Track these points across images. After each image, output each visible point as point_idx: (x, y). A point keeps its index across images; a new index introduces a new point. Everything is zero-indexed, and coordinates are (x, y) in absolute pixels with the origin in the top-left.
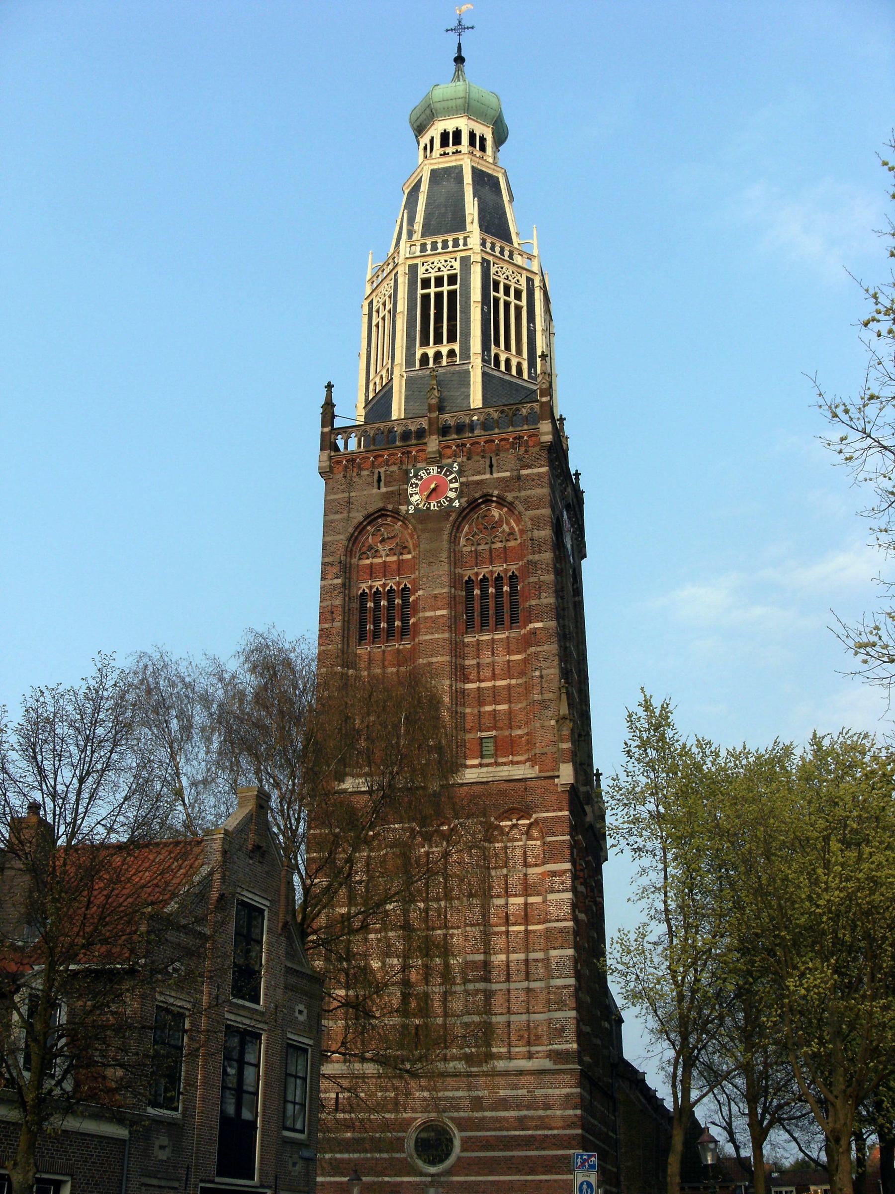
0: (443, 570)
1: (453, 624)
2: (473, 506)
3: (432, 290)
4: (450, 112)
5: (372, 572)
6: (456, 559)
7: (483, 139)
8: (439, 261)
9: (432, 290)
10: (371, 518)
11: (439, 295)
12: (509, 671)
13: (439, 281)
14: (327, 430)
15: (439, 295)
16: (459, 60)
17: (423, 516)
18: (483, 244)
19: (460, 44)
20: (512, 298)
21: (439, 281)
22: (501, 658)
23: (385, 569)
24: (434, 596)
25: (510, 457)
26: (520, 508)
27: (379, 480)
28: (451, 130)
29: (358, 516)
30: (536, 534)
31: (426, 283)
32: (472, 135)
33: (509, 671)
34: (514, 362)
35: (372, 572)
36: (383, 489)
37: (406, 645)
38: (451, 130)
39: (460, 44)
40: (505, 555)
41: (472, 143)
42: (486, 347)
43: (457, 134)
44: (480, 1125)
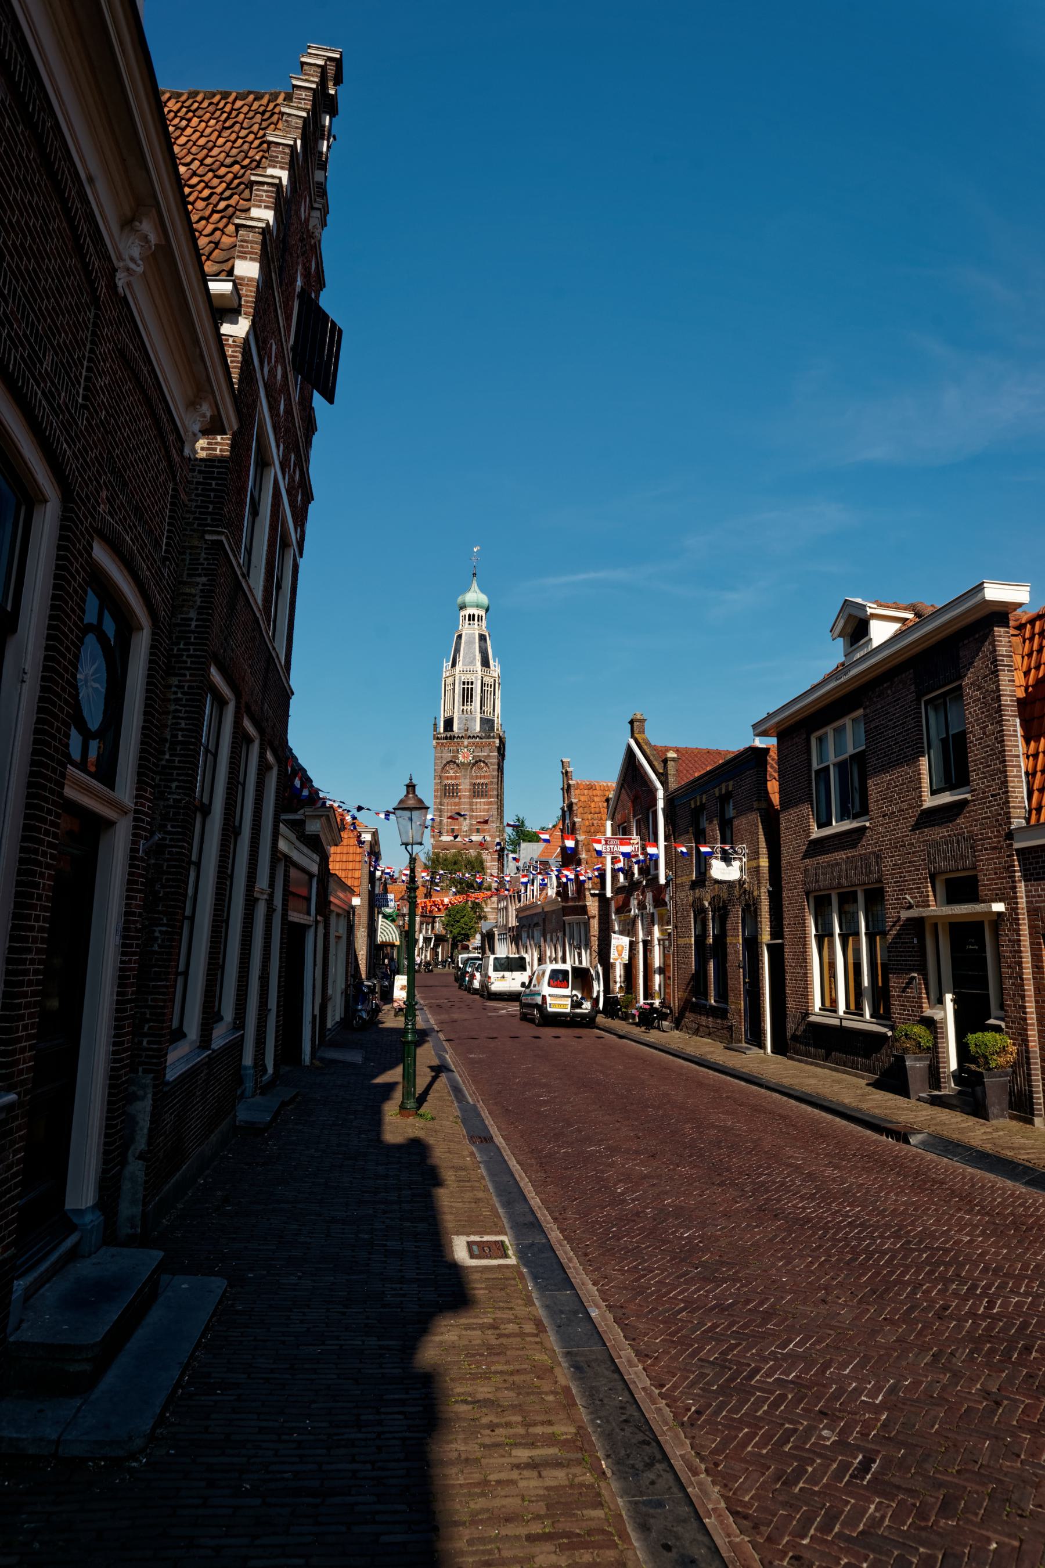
0: (468, 781)
1: (470, 797)
2: (476, 762)
4: (471, 606)
5: (448, 778)
6: (471, 778)
8: (468, 676)
10: (448, 763)
12: (484, 811)
17: (463, 764)
22: (483, 807)
23: (451, 778)
24: (465, 785)
25: (487, 749)
29: (445, 762)
31: (464, 683)
33: (484, 811)
35: (448, 778)
37: (457, 800)
40: (484, 777)
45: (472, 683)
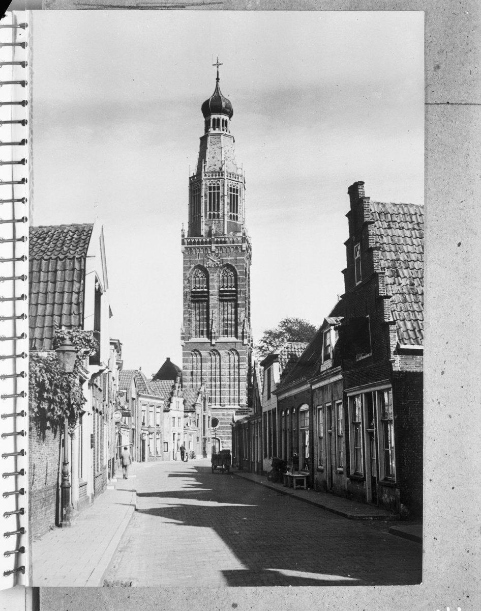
3: (212, 191)
7: (226, 121)
9: (212, 191)
11: (214, 193)
13: (214, 187)
14: (183, 238)
15: (214, 193)
16: (218, 79)
18: (228, 176)
19: (218, 72)
20: (235, 194)
21: (214, 190)
26: (236, 268)
27: (198, 256)
28: (216, 118)
30: (240, 277)
32: (223, 120)
34: (235, 215)
36: (200, 259)
38: (216, 118)
39: (218, 72)
41: (223, 126)
42: (228, 212)
43: (218, 119)
44: (224, 419)
45: (218, 188)
